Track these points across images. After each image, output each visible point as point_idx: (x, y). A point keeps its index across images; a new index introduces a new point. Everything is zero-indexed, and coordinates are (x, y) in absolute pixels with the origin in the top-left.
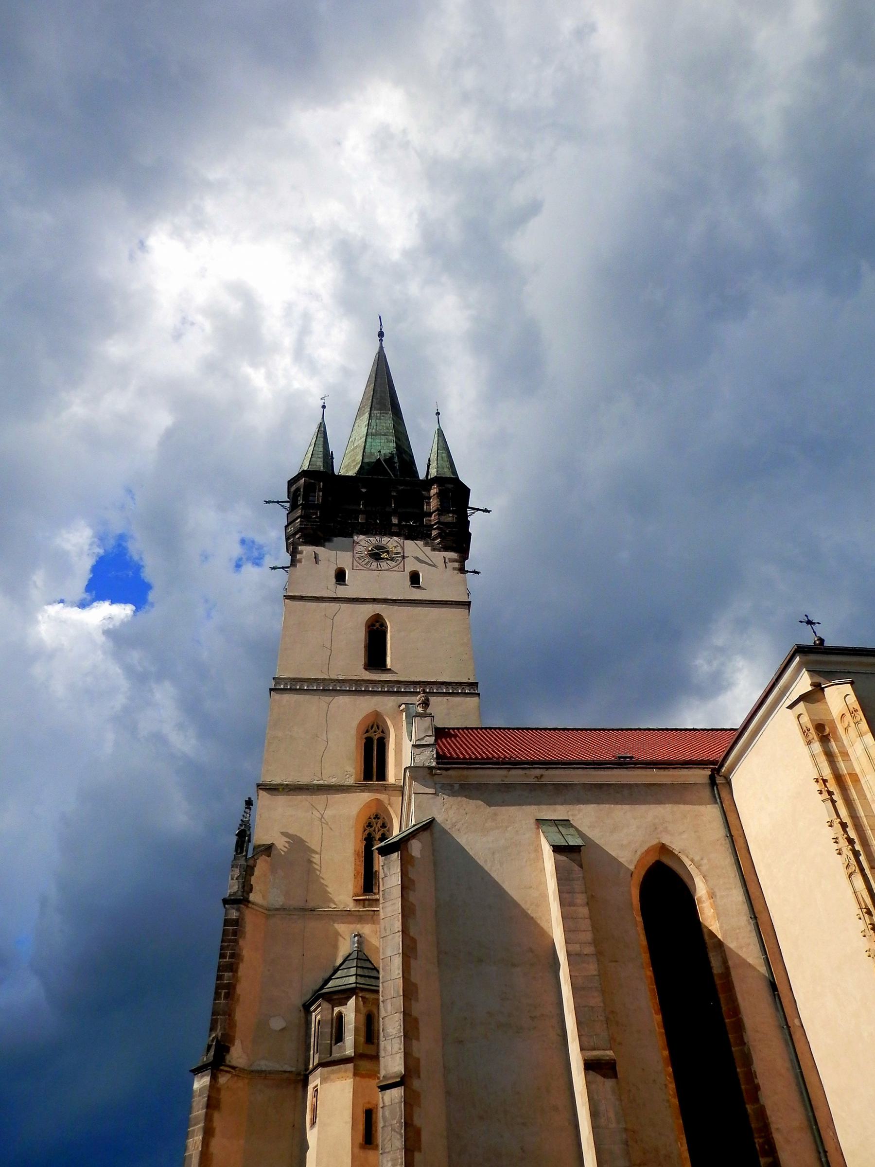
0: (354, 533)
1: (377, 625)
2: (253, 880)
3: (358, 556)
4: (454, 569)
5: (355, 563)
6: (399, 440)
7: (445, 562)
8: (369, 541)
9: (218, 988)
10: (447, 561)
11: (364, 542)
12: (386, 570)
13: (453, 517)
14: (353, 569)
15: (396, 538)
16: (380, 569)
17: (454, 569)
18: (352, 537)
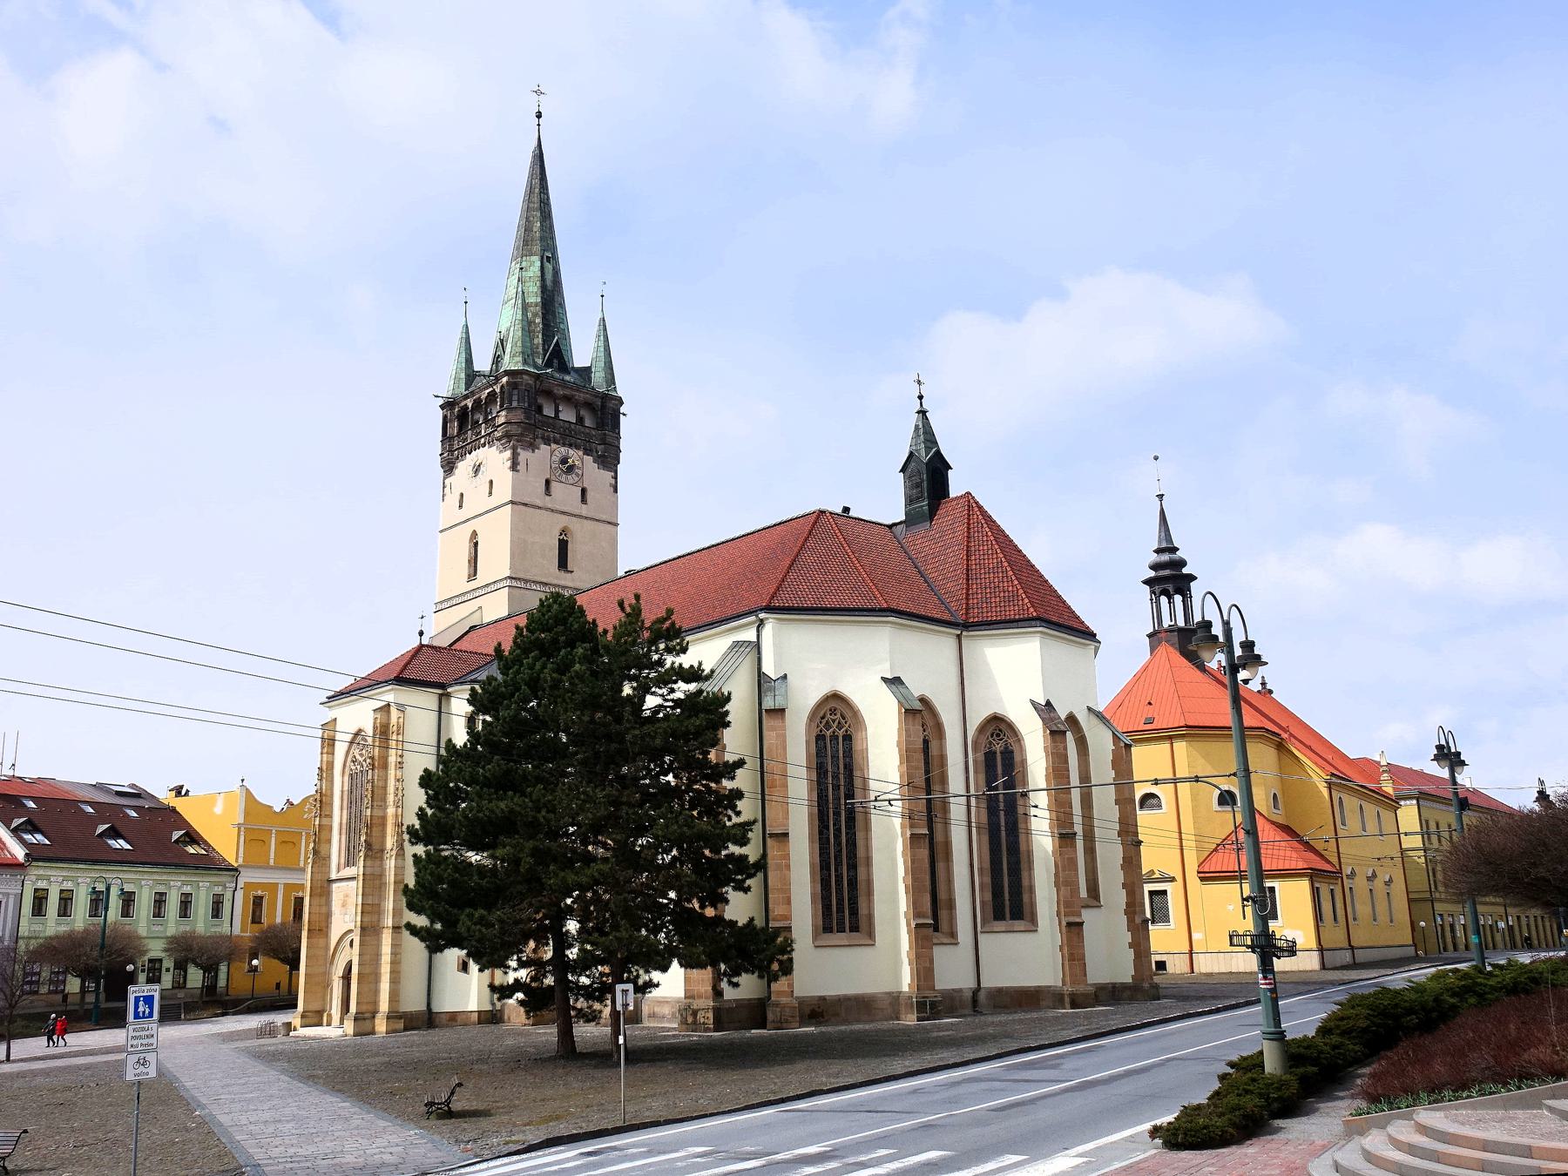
11: (471, 459)
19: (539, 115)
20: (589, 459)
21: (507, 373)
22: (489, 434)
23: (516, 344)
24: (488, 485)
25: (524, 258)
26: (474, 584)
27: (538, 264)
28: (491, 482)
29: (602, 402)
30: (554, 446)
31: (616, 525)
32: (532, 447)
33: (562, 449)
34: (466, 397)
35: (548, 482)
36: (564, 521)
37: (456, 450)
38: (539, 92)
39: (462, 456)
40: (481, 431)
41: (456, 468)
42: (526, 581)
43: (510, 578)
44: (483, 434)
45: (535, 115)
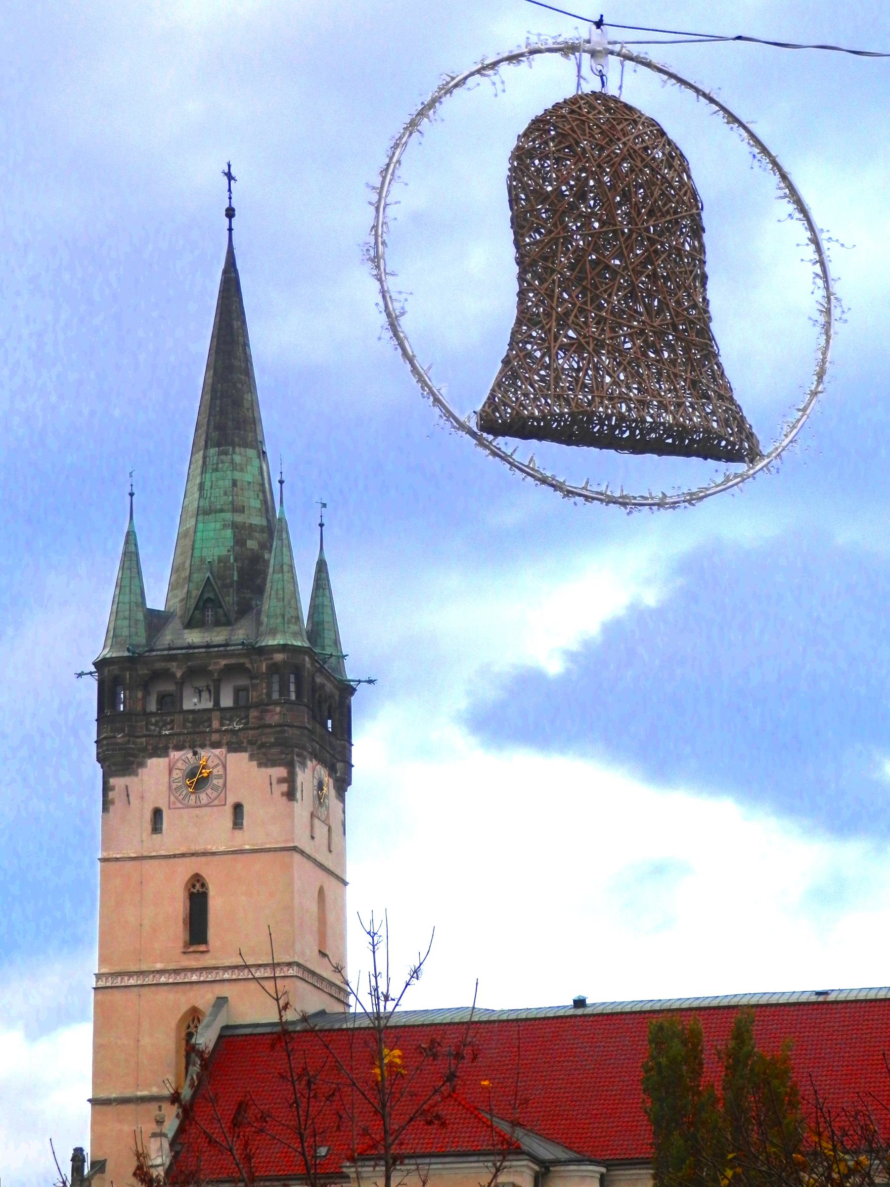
0: (168, 748)
1: (198, 886)
3: (174, 786)
4: (283, 794)
5: (172, 798)
6: (241, 510)
7: (271, 784)
8: (187, 761)
10: (274, 781)
12: (206, 805)
13: (280, 713)
14: (170, 808)
15: (217, 751)
16: (198, 804)
17: (283, 794)
18: (167, 755)
19: (230, 213)
20: (331, 781)
21: (284, 648)
22: (233, 732)
23: (290, 602)
24: (228, 811)
25: (237, 449)
27: (256, 462)
28: (238, 808)
29: (340, 697)
30: (314, 762)
31: (345, 883)
33: (319, 767)
37: (145, 736)
38: (229, 176)
40: (210, 720)
41: (142, 765)
43: (298, 965)
44: (216, 724)
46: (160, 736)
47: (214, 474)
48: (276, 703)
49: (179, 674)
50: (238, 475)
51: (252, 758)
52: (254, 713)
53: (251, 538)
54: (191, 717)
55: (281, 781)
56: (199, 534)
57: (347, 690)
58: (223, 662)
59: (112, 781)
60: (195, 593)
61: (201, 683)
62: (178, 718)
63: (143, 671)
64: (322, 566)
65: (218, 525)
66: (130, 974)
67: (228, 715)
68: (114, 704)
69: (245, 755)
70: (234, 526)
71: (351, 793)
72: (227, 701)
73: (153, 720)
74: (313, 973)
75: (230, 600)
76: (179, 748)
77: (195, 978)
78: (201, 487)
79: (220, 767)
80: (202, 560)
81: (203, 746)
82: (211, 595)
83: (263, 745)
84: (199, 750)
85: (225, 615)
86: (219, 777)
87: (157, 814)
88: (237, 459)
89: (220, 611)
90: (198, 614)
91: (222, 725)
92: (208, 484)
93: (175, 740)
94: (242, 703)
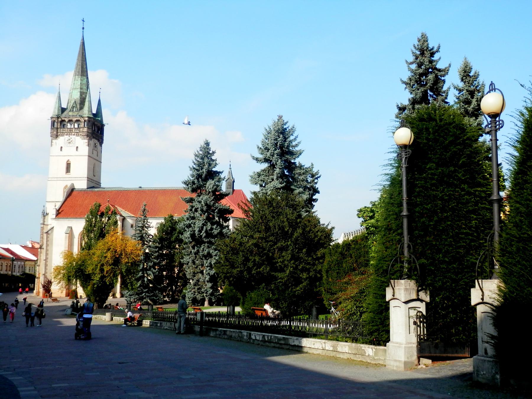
2: (45, 220)
9: (41, 237)
11: (66, 137)
19: (83, 28)
20: (98, 143)
21: (88, 117)
26: (68, 175)
32: (91, 140)
33: (95, 140)
34: (66, 118)
35: (93, 150)
36: (95, 161)
38: (83, 21)
39: (62, 135)
41: (59, 138)
42: (89, 178)
44: (74, 131)
45: (82, 28)
46: (63, 133)
47: (77, 81)
48: (86, 127)
49: (67, 121)
50: (82, 82)
51: (81, 137)
52: (81, 129)
53: (83, 94)
54: (69, 129)
55: (86, 143)
56: (73, 93)
57: (103, 126)
58: (76, 119)
59: (53, 141)
60: (72, 105)
61: (71, 123)
62: (66, 129)
63: (60, 120)
64: (99, 101)
65: (77, 92)
66: (55, 178)
67: (76, 129)
68: (54, 126)
69: (78, 138)
70: (81, 92)
71: (103, 145)
72: (76, 126)
73: (62, 129)
74: (92, 179)
75: (78, 107)
76: (66, 135)
77: (68, 179)
78: (74, 84)
79: (74, 140)
80: (73, 98)
81: (71, 135)
82: (75, 106)
83: (83, 136)
84: (70, 136)
85: (78, 110)
86: (74, 141)
87: (62, 147)
88: (82, 78)
89: (76, 109)
90: (72, 109)
91: (75, 131)
92: (75, 84)
93: (65, 134)
94: (80, 127)
